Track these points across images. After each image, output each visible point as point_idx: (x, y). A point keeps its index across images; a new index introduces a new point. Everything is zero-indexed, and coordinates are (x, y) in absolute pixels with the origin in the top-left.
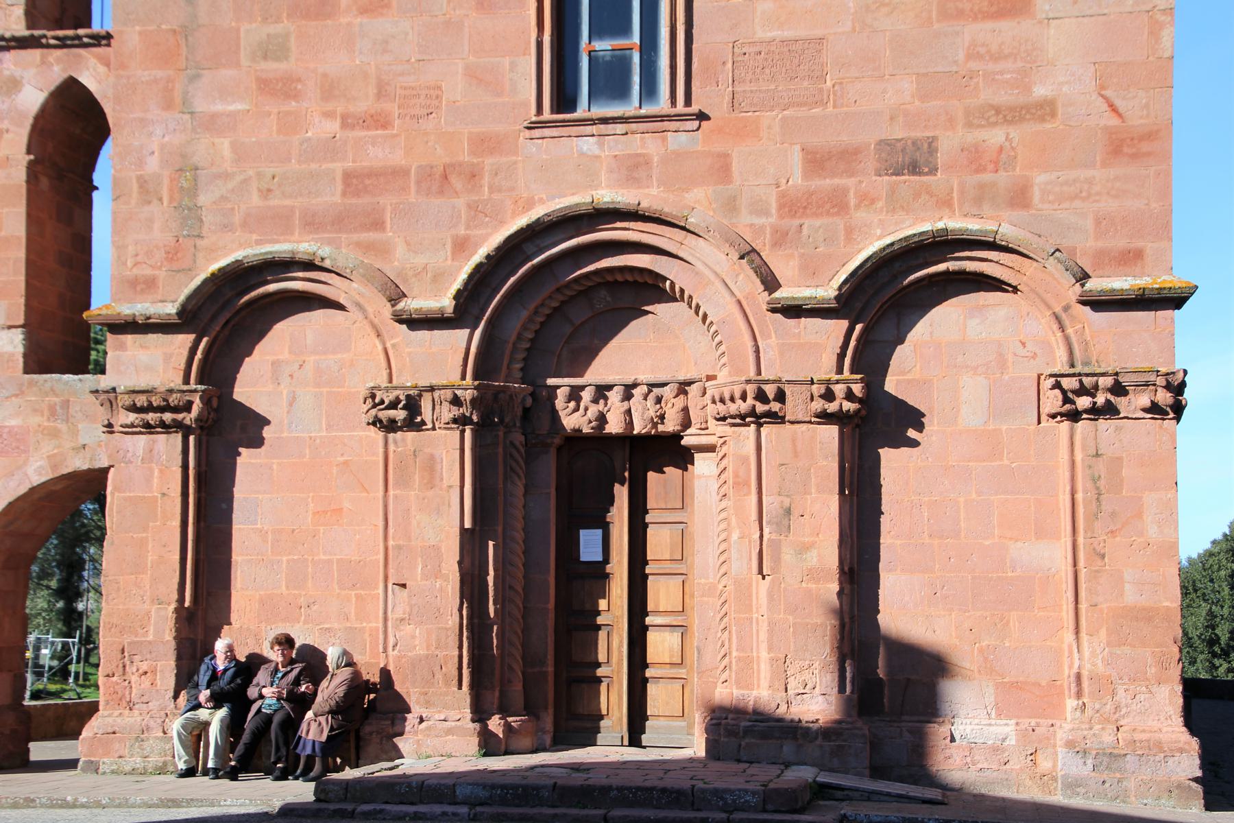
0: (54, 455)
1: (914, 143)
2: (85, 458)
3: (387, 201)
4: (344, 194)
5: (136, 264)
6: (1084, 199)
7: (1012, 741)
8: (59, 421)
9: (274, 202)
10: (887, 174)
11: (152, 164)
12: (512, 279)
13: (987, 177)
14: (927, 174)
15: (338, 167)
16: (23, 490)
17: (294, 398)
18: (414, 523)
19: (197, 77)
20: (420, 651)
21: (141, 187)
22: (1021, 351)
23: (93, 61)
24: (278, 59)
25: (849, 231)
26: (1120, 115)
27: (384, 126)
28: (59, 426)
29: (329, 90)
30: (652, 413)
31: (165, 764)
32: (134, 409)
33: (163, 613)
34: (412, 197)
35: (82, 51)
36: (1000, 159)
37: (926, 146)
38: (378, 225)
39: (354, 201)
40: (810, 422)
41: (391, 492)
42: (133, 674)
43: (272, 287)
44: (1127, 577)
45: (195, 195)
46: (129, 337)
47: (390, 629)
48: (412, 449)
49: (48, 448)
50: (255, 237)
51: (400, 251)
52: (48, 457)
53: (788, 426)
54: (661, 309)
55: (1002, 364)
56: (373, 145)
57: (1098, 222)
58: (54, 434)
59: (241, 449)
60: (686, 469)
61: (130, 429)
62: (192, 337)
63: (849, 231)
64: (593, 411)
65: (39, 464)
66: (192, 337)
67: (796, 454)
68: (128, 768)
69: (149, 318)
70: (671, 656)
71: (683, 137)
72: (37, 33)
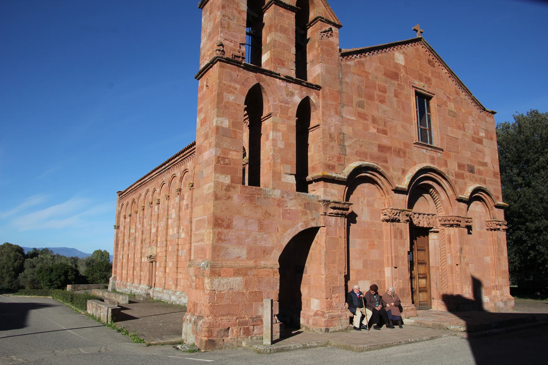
0: (305, 221)
2: (315, 223)
3: (388, 155)
4: (379, 151)
5: (329, 160)
6: (492, 184)
7: (489, 301)
9: (363, 149)
11: (333, 129)
12: (414, 183)
13: (481, 176)
15: (377, 142)
16: (297, 233)
17: (363, 209)
18: (399, 249)
19: (343, 106)
20: (401, 286)
21: (330, 136)
22: (482, 215)
23: (314, 94)
24: (362, 108)
25: (465, 183)
27: (386, 134)
28: (307, 211)
29: (374, 121)
30: (428, 222)
31: (347, 327)
32: (334, 208)
33: (341, 277)
35: (311, 89)
38: (386, 161)
39: (381, 153)
40: (464, 227)
41: (393, 240)
42: (334, 298)
43: (363, 174)
44: (503, 264)
45: (344, 142)
46: (329, 183)
47: (393, 280)
49: (304, 218)
50: (359, 158)
51: (391, 170)
52: (304, 221)
53: (460, 228)
54: (426, 195)
55: (481, 218)
56: (384, 138)
57: (494, 189)
58: (306, 214)
59: (351, 224)
60: (424, 237)
61: (331, 215)
62: (345, 186)
63: (465, 183)
64: (418, 220)
65: (301, 224)
66: (345, 186)
67: (462, 235)
68: (337, 330)
69: (339, 179)
70: (424, 285)
71: (440, 154)
72: (302, 80)
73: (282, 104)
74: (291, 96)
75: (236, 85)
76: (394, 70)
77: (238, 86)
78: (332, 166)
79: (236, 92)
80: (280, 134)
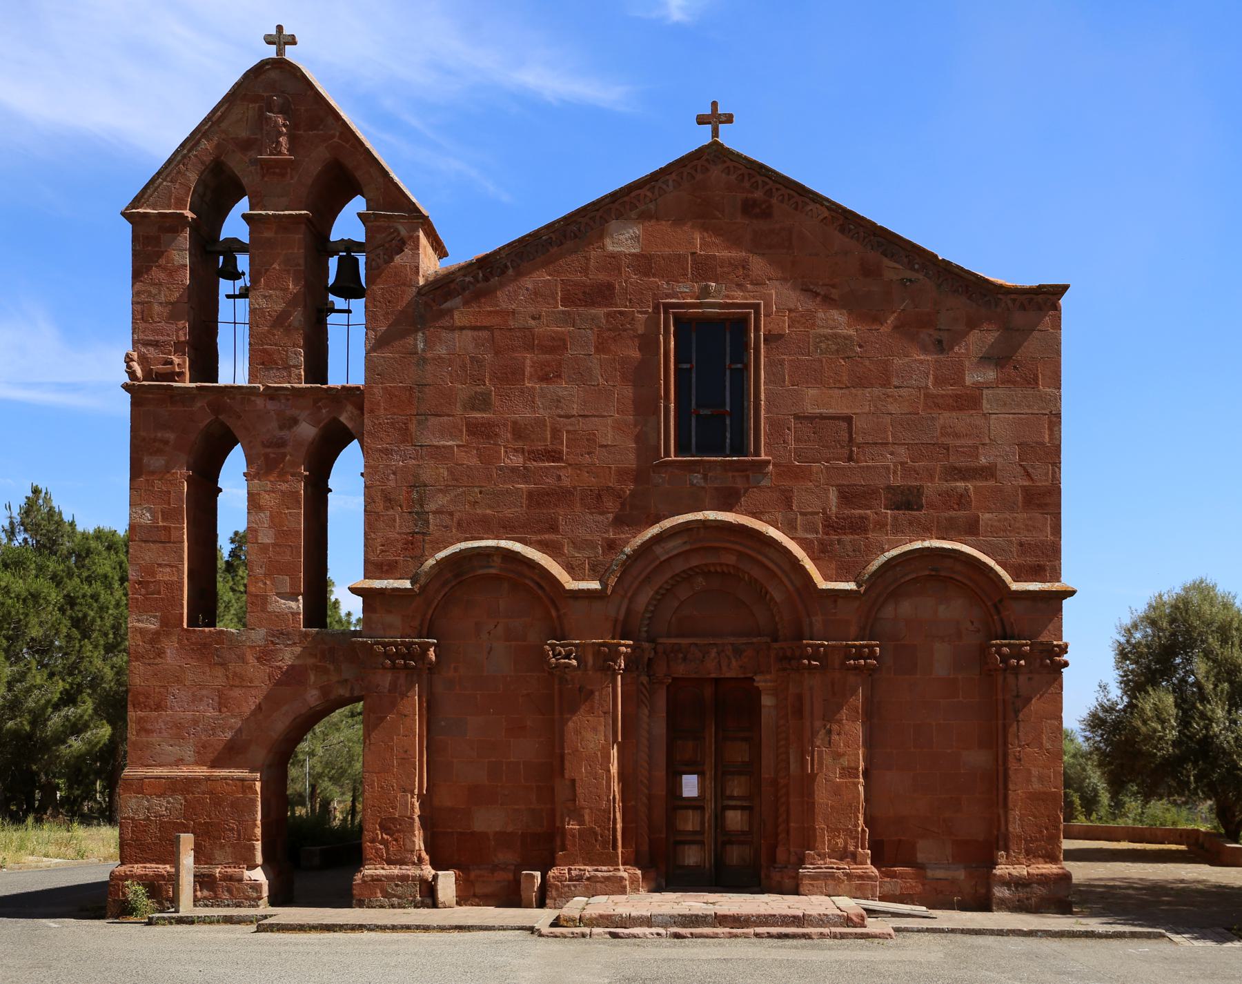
1: (909, 489)
4: (528, 507)
10: (892, 510)
13: (952, 513)
14: (917, 510)
26: (1032, 480)
29: (519, 432)
36: (962, 500)
37: (916, 491)
38: (554, 528)
73: (269, 450)
74: (290, 427)
75: (167, 435)
76: (602, 277)
77: (171, 436)
78: (389, 565)
80: (264, 516)
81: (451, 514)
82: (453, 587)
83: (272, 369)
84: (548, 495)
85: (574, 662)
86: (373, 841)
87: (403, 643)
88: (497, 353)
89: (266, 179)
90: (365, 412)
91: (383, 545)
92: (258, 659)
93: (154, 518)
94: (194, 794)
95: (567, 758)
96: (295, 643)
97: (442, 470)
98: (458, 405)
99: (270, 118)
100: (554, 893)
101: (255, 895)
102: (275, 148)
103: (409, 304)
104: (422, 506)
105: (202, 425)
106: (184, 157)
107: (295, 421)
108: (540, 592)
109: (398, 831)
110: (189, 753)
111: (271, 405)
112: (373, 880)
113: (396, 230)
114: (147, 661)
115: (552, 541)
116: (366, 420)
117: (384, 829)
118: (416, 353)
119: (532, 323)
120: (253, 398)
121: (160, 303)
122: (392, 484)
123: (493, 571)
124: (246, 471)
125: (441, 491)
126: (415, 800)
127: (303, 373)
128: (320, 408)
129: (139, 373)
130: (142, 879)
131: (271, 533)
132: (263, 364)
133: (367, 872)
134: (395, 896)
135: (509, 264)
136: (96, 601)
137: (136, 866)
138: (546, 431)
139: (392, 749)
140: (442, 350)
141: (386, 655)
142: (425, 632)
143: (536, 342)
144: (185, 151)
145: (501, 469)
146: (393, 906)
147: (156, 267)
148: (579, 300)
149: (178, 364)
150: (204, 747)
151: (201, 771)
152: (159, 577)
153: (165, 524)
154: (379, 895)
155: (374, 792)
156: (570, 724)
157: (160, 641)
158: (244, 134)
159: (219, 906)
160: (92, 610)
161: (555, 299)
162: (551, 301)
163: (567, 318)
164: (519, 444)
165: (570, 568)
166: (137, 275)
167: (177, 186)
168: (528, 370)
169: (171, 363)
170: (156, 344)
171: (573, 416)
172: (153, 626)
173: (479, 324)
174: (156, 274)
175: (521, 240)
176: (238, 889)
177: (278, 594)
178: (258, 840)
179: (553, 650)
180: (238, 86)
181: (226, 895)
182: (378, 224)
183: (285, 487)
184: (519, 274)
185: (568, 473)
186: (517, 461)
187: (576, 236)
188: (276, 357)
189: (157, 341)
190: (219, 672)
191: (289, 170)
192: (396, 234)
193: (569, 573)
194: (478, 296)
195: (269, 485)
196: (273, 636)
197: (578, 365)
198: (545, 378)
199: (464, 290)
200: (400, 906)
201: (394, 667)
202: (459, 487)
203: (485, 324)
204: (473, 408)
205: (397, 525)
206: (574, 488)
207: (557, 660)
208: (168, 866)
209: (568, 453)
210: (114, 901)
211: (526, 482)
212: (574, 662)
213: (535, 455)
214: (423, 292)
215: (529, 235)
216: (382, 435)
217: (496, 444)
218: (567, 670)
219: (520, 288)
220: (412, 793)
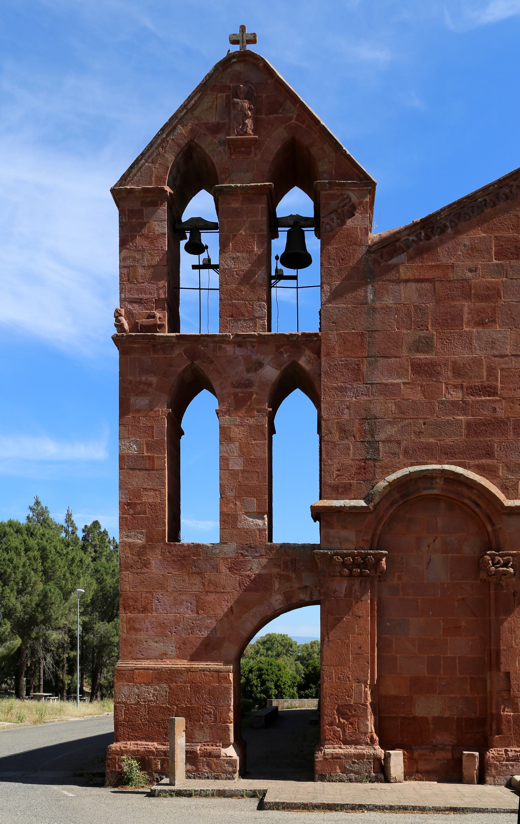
8: (290, 571)
34: (511, 436)
48: (512, 591)
73: (238, 390)
74: (256, 370)
77: (153, 379)
79: (151, 390)
81: (399, 443)
82: (400, 505)
83: (240, 320)
84: (484, 425)
85: (511, 570)
86: (331, 724)
87: (359, 554)
88: (437, 302)
89: (233, 157)
90: (322, 355)
91: (339, 470)
92: (230, 569)
93: (140, 449)
94: (176, 683)
95: (503, 653)
96: (261, 555)
97: (390, 405)
98: (404, 348)
99: (238, 103)
100: (493, 771)
101: (231, 769)
102: (242, 129)
103: (360, 261)
104: (373, 436)
105: (180, 370)
106: (163, 140)
107: (260, 365)
108: (477, 510)
109: (354, 716)
110: (171, 649)
111: (239, 352)
112: (333, 758)
113: (348, 197)
114: (135, 571)
115: (488, 465)
116: (323, 363)
117: (341, 714)
118: (367, 303)
119: (469, 275)
120: (224, 346)
121: (144, 267)
122: (346, 417)
123: (436, 492)
124: (218, 408)
125: (389, 422)
126: (368, 689)
127: (266, 323)
128: (281, 353)
129: (126, 326)
130: (134, 754)
131: (240, 461)
132: (232, 316)
133: (327, 751)
134: (352, 772)
135: (448, 224)
136: (12, 563)
137: (129, 743)
138: (482, 369)
139: (348, 646)
140: (389, 301)
141: (344, 564)
142: (375, 545)
143: (473, 292)
144: (164, 136)
145: (442, 403)
146: (350, 781)
147: (140, 236)
148: (512, 254)
149: (160, 318)
150: (184, 643)
151: (183, 664)
152: (144, 499)
153: (149, 454)
154: (338, 770)
155: (332, 682)
156: (506, 624)
157: (146, 553)
158: (213, 119)
159: (200, 778)
160: (9, 568)
161: (489, 253)
162: (486, 256)
163: (500, 270)
164: (459, 381)
165: (504, 489)
166: (123, 243)
167: (157, 166)
168: (466, 317)
169: (154, 317)
170: (139, 302)
171: (507, 356)
172: (140, 541)
173: (421, 277)
174: (139, 241)
175: (460, 203)
176: (216, 764)
177: (246, 513)
178: (231, 723)
179: (493, 560)
180: (210, 77)
181: (206, 769)
182: (332, 192)
183: (251, 421)
184: (457, 232)
185: (502, 405)
186: (456, 395)
187: (507, 198)
188: (243, 309)
189: (141, 299)
190: (197, 580)
191: (253, 149)
192: (348, 200)
193: (503, 493)
194: (421, 252)
195: (238, 420)
196: (243, 549)
197: (510, 310)
198: (481, 323)
199: (408, 247)
200: (357, 781)
201: (351, 575)
202: (405, 419)
203: (427, 277)
204: (418, 351)
205: (351, 452)
206: (508, 418)
207: (496, 568)
208: (155, 743)
209: (502, 388)
210: (112, 772)
211: (465, 414)
212: (511, 570)
213: (473, 391)
214: (373, 249)
215: (468, 197)
216: (338, 375)
217: (438, 381)
218: (503, 577)
219: (458, 244)
220: (366, 683)
